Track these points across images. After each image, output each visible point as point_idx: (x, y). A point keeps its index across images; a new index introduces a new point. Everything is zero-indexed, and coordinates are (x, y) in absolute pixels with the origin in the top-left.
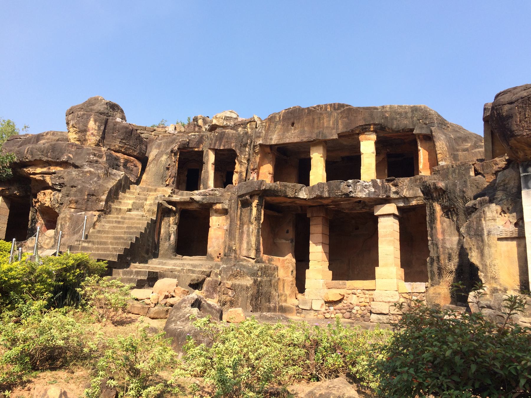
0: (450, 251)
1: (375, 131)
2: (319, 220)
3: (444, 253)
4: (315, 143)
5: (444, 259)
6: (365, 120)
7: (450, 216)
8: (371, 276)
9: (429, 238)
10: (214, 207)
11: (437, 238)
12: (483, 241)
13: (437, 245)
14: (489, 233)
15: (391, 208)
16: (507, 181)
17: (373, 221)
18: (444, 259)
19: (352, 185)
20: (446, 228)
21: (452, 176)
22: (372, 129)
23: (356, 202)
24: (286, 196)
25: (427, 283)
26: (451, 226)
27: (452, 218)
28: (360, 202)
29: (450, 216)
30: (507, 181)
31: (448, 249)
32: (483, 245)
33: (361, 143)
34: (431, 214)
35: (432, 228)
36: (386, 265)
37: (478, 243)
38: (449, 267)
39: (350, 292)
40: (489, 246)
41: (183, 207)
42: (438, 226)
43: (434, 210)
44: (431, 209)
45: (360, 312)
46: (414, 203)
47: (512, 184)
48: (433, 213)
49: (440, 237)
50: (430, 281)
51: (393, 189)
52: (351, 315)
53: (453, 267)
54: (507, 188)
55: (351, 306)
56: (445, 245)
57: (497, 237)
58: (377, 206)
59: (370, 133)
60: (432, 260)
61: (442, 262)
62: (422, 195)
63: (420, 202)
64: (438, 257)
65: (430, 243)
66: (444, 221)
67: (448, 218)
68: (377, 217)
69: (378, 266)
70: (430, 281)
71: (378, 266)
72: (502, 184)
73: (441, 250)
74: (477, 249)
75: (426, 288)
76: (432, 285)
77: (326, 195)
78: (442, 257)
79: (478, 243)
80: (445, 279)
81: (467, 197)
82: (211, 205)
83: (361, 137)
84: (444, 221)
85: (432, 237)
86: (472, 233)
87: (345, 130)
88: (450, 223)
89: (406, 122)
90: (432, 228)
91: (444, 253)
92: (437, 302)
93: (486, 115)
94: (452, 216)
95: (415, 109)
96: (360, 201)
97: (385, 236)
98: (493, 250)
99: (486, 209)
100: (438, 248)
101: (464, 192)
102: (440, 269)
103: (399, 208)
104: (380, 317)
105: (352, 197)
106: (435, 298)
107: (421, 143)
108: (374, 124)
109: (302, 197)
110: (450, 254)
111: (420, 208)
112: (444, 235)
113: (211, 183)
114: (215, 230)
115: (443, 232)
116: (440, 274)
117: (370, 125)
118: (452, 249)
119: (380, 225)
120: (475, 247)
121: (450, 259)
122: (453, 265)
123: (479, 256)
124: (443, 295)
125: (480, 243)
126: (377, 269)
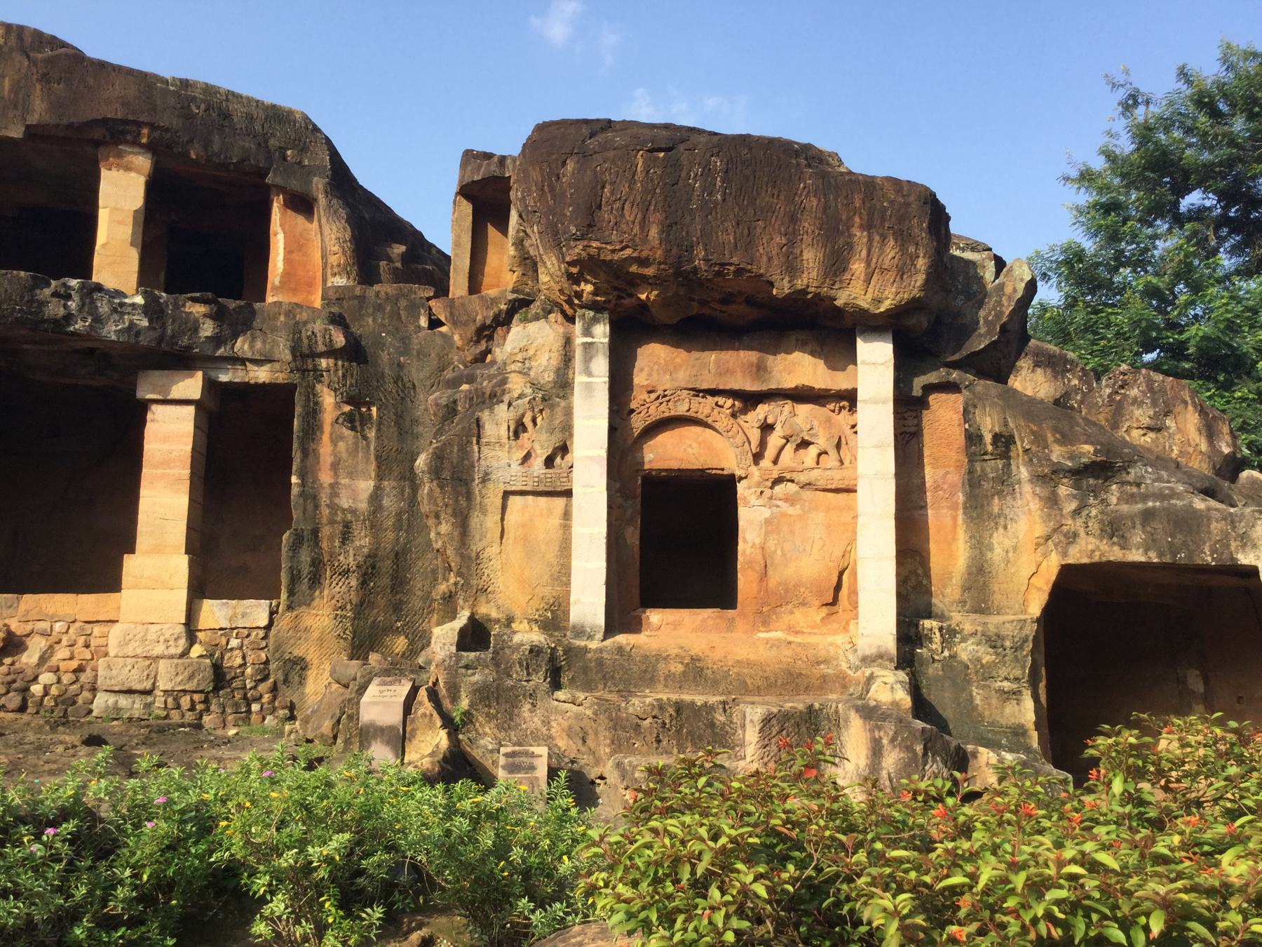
0: (349, 517)
1: (151, 148)
3: (332, 522)
5: (331, 539)
6: (125, 104)
7: (357, 424)
8: (109, 581)
9: (294, 479)
11: (316, 480)
12: (469, 496)
14: (485, 479)
15: (191, 386)
16: (531, 352)
17: (133, 418)
18: (331, 539)
19: (76, 297)
20: (344, 455)
21: (374, 320)
22: (144, 141)
23: (77, 351)
25: (274, 603)
26: (356, 450)
27: (363, 430)
28: (95, 353)
29: (357, 424)
30: (531, 352)
31: (344, 510)
32: (469, 508)
33: (104, 173)
34: (308, 413)
35: (305, 453)
36: (158, 549)
37: (457, 501)
38: (341, 558)
39: (29, 627)
40: (484, 511)
42: (325, 449)
43: (316, 403)
44: (308, 400)
45: (54, 691)
46: (261, 375)
47: (544, 362)
48: (315, 411)
49: (325, 478)
50: (284, 596)
51: (208, 329)
52: (25, 701)
53: (351, 559)
54: (529, 369)
55: (29, 674)
56: (337, 501)
57: (502, 488)
58: (150, 372)
59: (136, 150)
61: (324, 545)
62: (287, 356)
63: (281, 378)
64: (315, 532)
65: (295, 491)
66: (342, 438)
67: (353, 428)
68: (144, 406)
69: (132, 550)
70: (284, 596)
71: (132, 550)
72: (519, 357)
73: (326, 512)
74: (454, 514)
75: (272, 613)
76: (290, 608)
78: (326, 531)
79: (457, 501)
80: (326, 592)
81: (406, 379)
83: (102, 151)
84: (342, 438)
85: (302, 476)
86: (446, 474)
87: (47, 118)
88: (356, 444)
89: (249, 144)
90: (305, 453)
91: (332, 522)
92: (297, 653)
93: (467, 180)
94: (362, 425)
95: (277, 115)
96: (92, 351)
97: (166, 463)
98: (491, 521)
99: (485, 416)
100: (317, 507)
101: (399, 365)
102: (317, 564)
104: (124, 701)
105: (73, 334)
106: (292, 641)
107: (283, 214)
108: (152, 126)
110: (347, 526)
111: (279, 395)
112: (336, 475)
115: (335, 467)
116: (316, 581)
117: (140, 125)
118: (353, 511)
119: (151, 430)
120: (450, 511)
121: (346, 536)
122: (351, 553)
123: (456, 533)
124: (316, 634)
125: (463, 503)
126: (132, 565)
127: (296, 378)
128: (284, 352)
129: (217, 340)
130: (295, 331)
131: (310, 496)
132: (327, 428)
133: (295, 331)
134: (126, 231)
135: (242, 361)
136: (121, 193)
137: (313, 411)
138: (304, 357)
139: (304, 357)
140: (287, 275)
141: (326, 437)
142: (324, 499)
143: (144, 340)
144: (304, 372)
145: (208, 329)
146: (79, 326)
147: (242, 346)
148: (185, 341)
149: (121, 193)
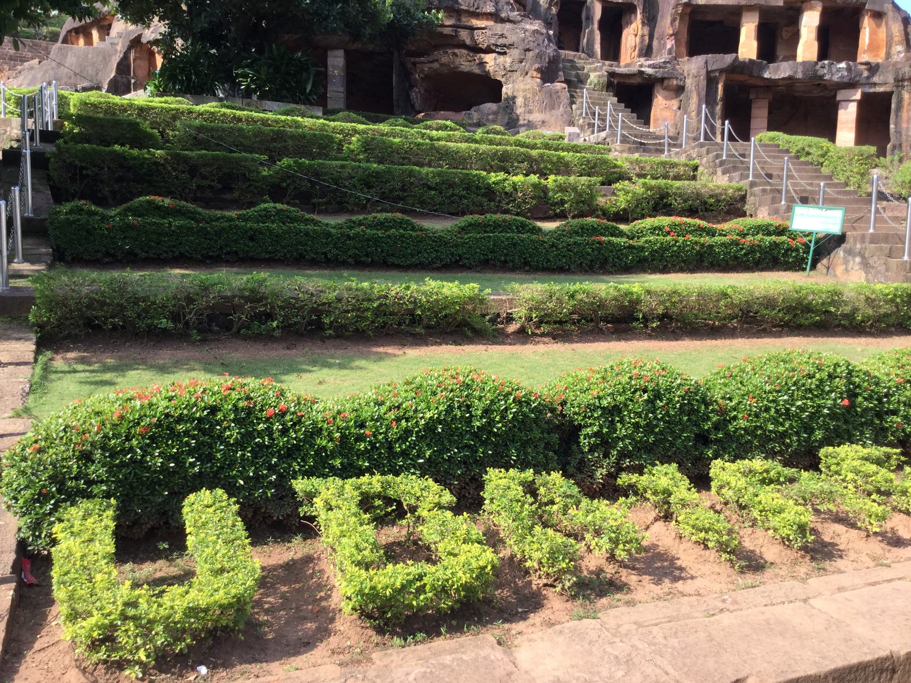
2: (765, 103)
4: (750, 8)
9: (892, 126)
10: (666, 83)
13: (900, 132)
24: (751, 75)
35: (897, 116)
41: (622, 81)
46: (881, 89)
49: (904, 125)
51: (866, 74)
60: (894, 148)
64: (900, 145)
73: (904, 137)
77: (800, 76)
82: (662, 80)
85: (896, 124)
97: (846, 122)
103: (864, 95)
109: (766, 76)
111: (887, 96)
113: (598, 48)
114: (662, 110)
127: (895, 89)
128: (891, 80)
129: (868, 78)
130: (897, 71)
131: (898, 132)
132: (905, 106)
133: (897, 71)
134: (813, 35)
135: (875, 84)
136: (810, 21)
137: (900, 102)
138: (899, 81)
139: (899, 81)
140: (870, 45)
141: (905, 110)
142: (904, 133)
143: (845, 80)
144: (897, 86)
145: (866, 74)
146: (827, 77)
147: (876, 79)
148: (857, 79)
149: (810, 21)
